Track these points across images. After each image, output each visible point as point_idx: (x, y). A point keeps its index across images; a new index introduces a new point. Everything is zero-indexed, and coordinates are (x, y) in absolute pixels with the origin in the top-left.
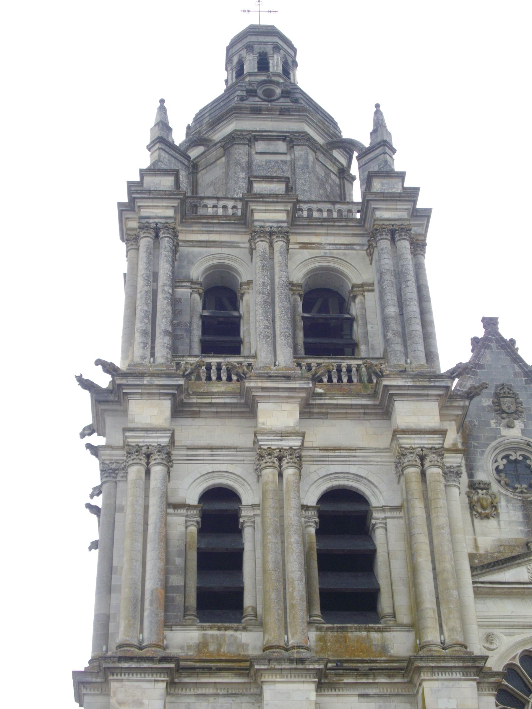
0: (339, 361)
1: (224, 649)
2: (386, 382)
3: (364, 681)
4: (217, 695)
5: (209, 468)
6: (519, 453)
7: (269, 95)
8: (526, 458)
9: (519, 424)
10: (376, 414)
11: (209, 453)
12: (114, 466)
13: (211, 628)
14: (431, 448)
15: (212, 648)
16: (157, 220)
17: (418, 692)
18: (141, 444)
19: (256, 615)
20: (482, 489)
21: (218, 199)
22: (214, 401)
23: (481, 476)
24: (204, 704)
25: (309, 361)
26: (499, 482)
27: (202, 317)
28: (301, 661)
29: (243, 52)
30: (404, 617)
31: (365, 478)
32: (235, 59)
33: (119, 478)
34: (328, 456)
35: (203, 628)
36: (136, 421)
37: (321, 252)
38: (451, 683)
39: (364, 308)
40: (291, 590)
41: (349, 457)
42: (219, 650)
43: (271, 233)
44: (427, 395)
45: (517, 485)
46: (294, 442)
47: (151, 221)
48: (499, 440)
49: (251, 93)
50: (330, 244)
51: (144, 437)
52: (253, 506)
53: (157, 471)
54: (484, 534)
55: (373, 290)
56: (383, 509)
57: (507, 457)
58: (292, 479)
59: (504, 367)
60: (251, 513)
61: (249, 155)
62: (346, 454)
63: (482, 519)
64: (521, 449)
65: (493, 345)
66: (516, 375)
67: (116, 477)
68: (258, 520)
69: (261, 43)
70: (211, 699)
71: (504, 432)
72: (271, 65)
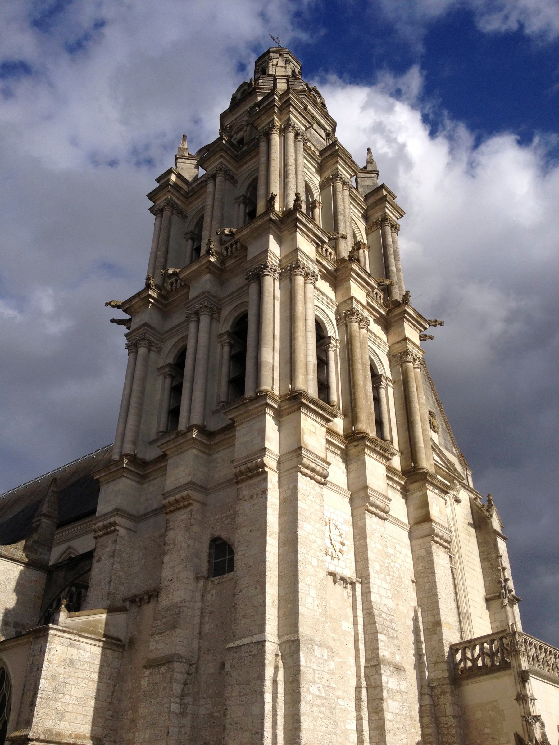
2: (407, 309)
22: (324, 263)
31: (378, 356)
40: (369, 403)
41: (374, 339)
44: (417, 328)
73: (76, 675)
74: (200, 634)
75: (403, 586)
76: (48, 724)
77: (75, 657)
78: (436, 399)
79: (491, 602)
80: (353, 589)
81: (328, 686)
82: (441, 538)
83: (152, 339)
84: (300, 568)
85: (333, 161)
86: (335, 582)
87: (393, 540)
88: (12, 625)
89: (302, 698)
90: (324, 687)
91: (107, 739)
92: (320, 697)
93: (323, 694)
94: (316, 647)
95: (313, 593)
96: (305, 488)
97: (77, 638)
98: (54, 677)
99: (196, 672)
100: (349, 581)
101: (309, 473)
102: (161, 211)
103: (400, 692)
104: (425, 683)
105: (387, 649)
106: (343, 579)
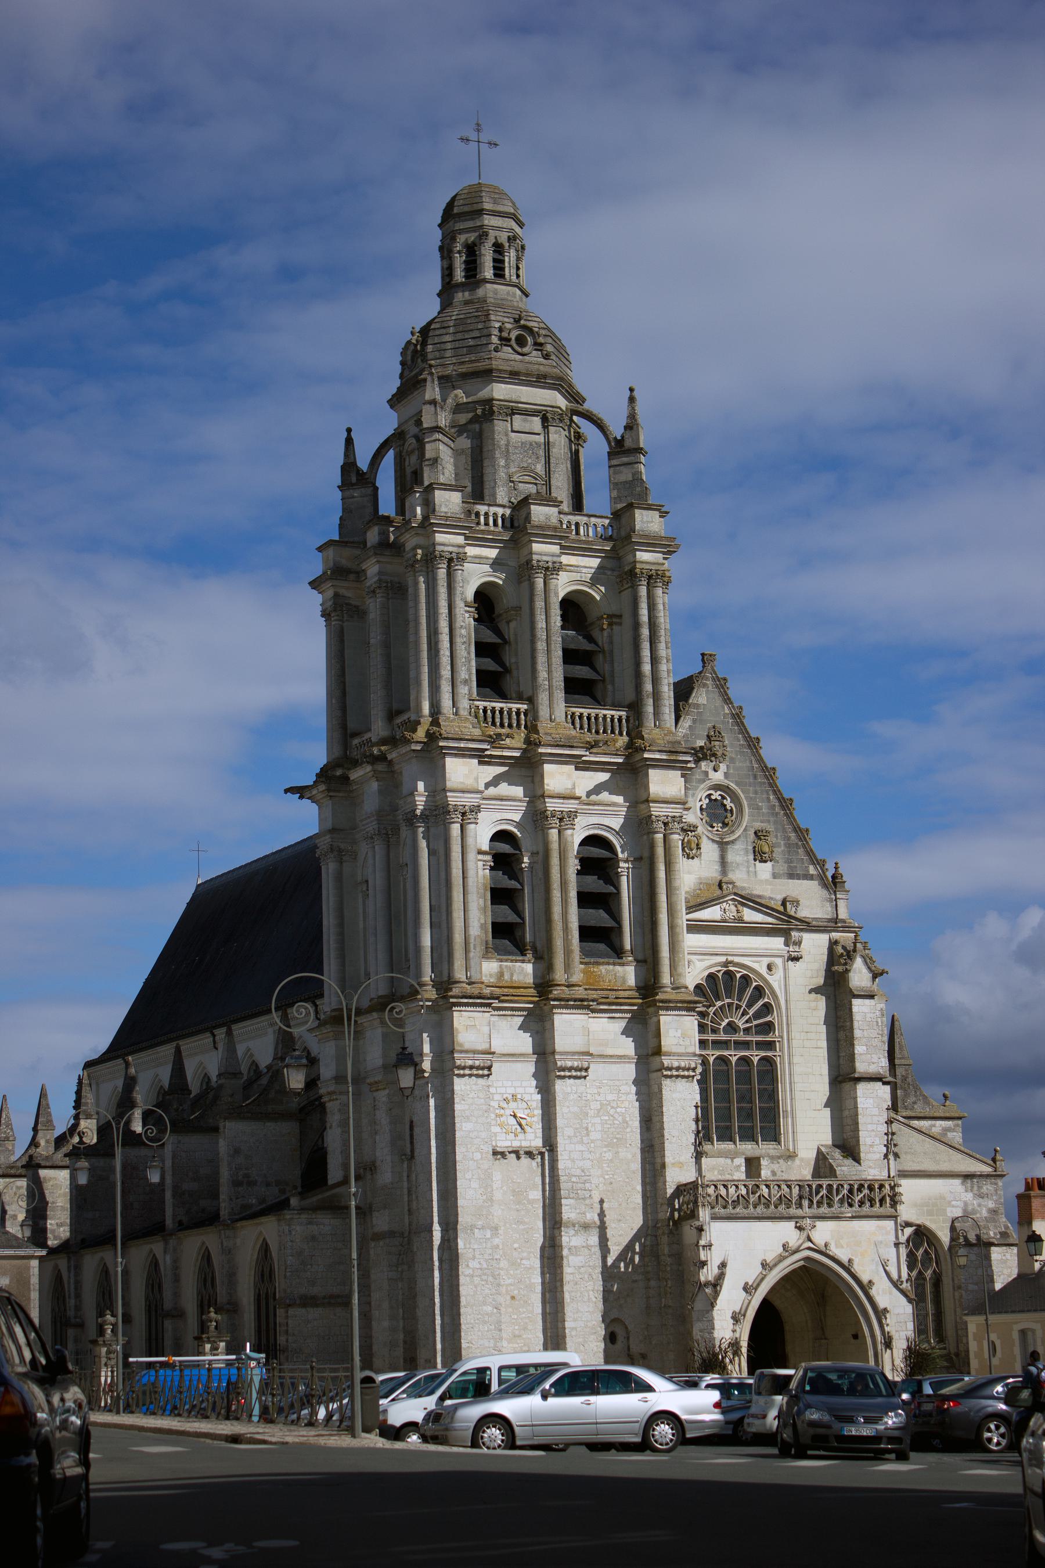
0: (597, 711)
1: (515, 978)
2: (646, 755)
3: (614, 1007)
6: (719, 793)
9: (723, 767)
10: (627, 769)
11: (499, 803)
13: (506, 961)
14: (674, 817)
15: (507, 977)
16: (450, 549)
17: (650, 1018)
20: (691, 831)
23: (692, 817)
26: (702, 820)
28: (582, 1000)
34: (589, 809)
37: (577, 576)
38: (678, 1018)
39: (611, 643)
42: (511, 979)
43: (547, 569)
45: (715, 825)
46: (571, 805)
47: (446, 549)
48: (707, 782)
49: (505, 341)
50: (585, 567)
51: (461, 797)
54: (689, 873)
55: (620, 624)
57: (710, 795)
61: (507, 435)
63: (688, 858)
64: (721, 790)
65: (709, 682)
66: (725, 715)
67: (427, 823)
71: (712, 775)
72: (507, 264)
74: (409, 1210)
75: (628, 1130)
78: (778, 799)
80: (543, 1158)
81: (492, 1259)
82: (678, 1069)
83: (342, 846)
84: (458, 1167)
85: (526, 539)
86: (518, 1158)
87: (617, 1083)
89: (460, 1273)
90: (486, 1261)
92: (481, 1269)
93: (485, 1266)
94: (476, 1231)
95: (475, 1184)
96: (463, 1088)
97: (314, 1216)
99: (409, 1243)
101: (467, 1072)
102: (329, 615)
103: (588, 1247)
105: (573, 1210)
106: (530, 1154)
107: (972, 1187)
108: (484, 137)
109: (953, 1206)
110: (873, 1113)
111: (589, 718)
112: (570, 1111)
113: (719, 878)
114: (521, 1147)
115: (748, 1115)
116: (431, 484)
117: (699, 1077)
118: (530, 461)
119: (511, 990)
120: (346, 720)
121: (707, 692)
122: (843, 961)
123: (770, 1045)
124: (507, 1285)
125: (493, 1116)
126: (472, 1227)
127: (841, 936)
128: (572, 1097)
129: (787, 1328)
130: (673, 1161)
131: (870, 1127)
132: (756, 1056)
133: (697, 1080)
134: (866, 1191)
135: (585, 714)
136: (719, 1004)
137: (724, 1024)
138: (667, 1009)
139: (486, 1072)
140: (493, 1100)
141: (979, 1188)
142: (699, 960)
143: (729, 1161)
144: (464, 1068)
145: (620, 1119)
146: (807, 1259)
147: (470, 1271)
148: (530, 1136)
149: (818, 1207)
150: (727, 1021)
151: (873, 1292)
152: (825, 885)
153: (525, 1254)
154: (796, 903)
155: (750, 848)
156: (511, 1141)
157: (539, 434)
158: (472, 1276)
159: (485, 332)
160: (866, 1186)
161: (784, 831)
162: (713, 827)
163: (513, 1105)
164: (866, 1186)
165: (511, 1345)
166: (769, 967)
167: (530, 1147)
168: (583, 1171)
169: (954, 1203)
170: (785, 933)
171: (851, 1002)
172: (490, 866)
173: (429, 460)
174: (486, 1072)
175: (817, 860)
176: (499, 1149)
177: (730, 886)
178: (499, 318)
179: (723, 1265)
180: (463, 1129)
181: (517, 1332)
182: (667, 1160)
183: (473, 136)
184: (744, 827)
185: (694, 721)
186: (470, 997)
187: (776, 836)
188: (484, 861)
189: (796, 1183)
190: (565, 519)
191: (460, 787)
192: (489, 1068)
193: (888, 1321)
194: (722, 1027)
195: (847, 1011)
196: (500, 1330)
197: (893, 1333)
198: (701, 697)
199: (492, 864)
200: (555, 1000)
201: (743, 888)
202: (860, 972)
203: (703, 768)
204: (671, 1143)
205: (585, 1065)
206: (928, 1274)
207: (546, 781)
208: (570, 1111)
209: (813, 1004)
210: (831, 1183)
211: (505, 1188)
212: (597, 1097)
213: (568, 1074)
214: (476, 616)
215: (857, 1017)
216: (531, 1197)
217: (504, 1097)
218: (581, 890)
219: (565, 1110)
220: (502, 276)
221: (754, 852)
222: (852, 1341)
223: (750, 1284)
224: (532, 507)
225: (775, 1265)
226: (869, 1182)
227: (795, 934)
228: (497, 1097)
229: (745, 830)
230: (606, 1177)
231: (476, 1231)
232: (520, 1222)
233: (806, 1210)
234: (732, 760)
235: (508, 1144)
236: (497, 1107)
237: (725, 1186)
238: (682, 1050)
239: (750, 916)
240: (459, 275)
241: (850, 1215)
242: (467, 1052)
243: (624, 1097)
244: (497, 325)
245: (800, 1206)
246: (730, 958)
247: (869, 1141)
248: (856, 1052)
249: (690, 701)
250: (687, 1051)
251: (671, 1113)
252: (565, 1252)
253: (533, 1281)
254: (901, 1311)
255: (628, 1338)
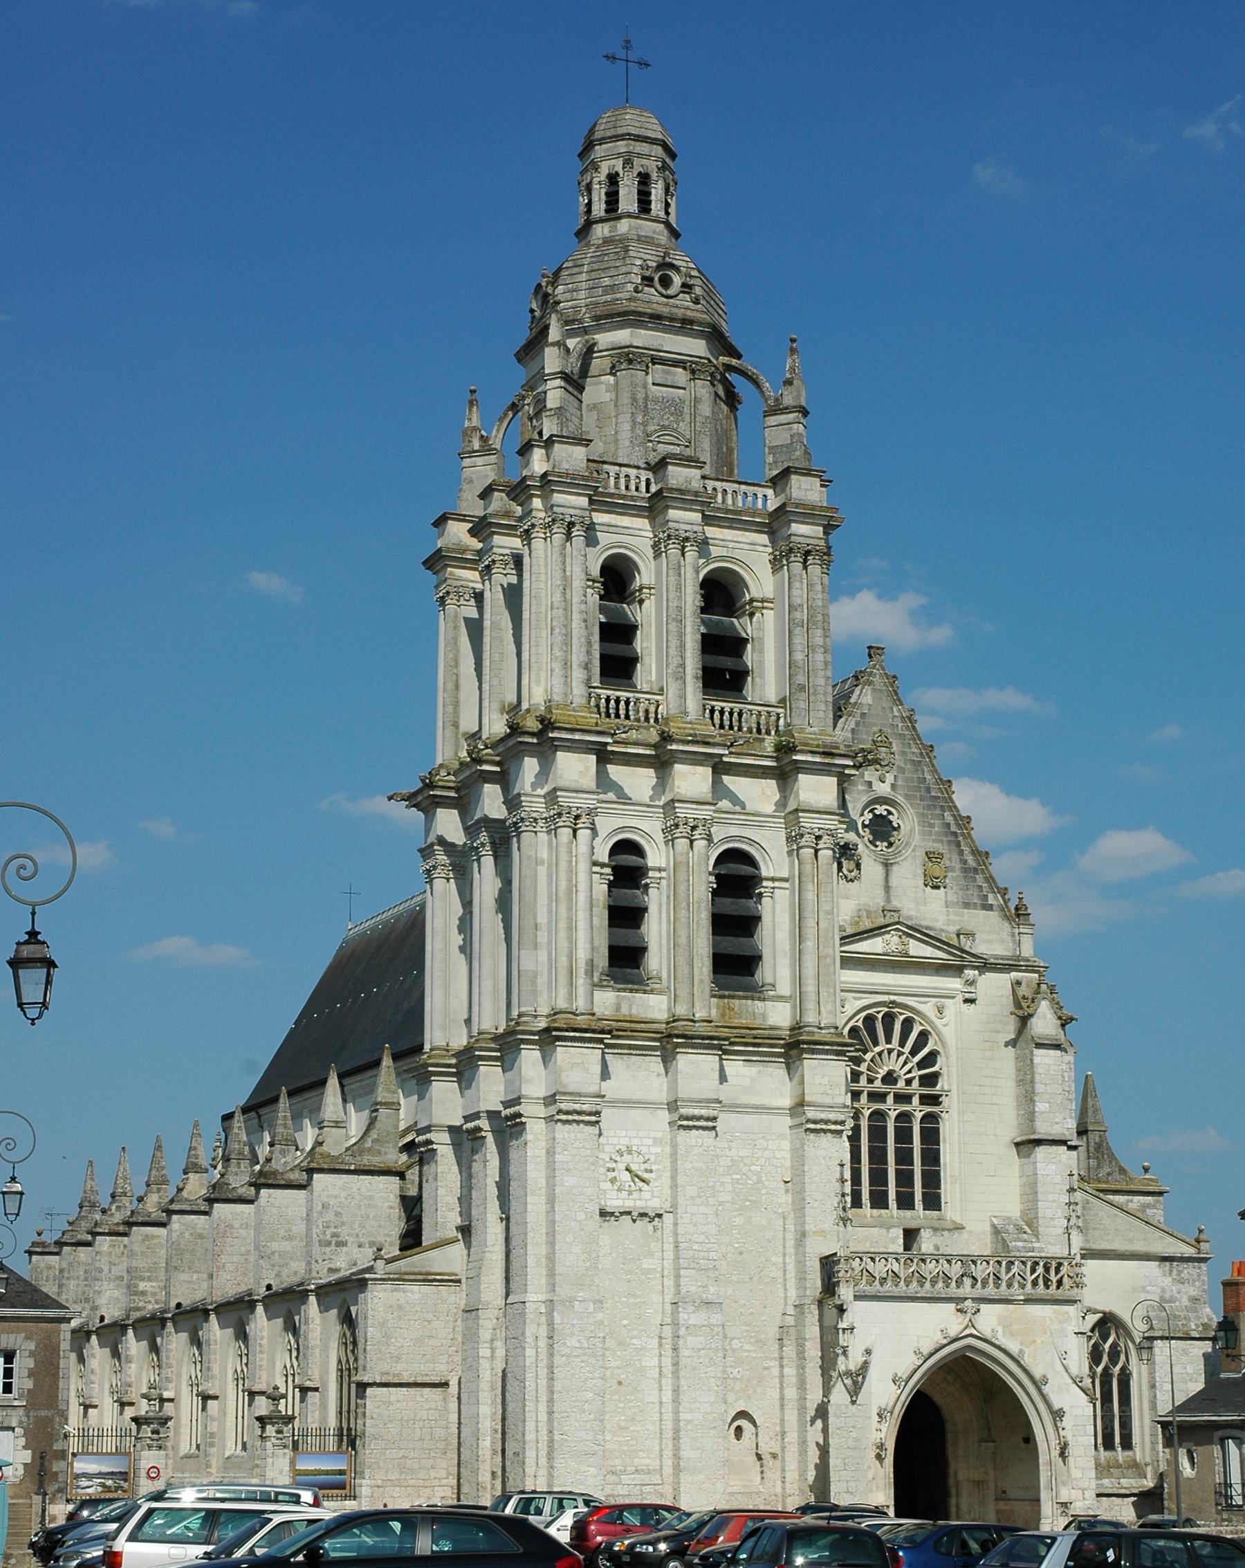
1: (634, 1011)
4: (631, 1054)
5: (621, 822)
7: (666, 282)
8: (890, 813)
12: (534, 815)
16: (572, 511)
18: (571, 805)
19: (660, 979)
21: (621, 465)
24: (620, 1061)
25: (714, 703)
27: (601, 623)
29: (618, 165)
30: (784, 988)
32: (605, 169)
33: (538, 829)
35: (619, 990)
36: (565, 777)
43: (687, 539)
45: (878, 843)
49: (648, 281)
52: (660, 870)
53: (584, 834)
56: (773, 879)
58: (703, 851)
59: (884, 708)
60: (657, 875)
61: (645, 387)
62: (745, 817)
64: (887, 804)
68: (664, 882)
69: (640, 156)
70: (625, 1057)
72: (653, 197)
73: (406, 1318)
75: (764, 1191)
76: (385, 1367)
77: (402, 1301)
78: (954, 816)
79: (1022, 1147)
88: (367, 1245)
91: (453, 1373)
92: (580, 1348)
98: (382, 1324)
100: (652, 1214)
103: (709, 1326)
104: (790, 1302)
107: (1171, 1271)
108: (633, 56)
109: (1148, 1292)
110: (1056, 1181)
111: (731, 714)
112: (693, 1167)
113: (882, 904)
114: (635, 1208)
115: (905, 1179)
116: (552, 436)
117: (850, 1133)
118: (672, 419)
119: (628, 1025)
120: (458, 717)
121: (874, 690)
122: (1024, 1004)
123: (934, 1100)
124: (613, 1368)
125: (603, 1170)
126: (571, 1301)
127: (1022, 977)
128: (696, 1151)
129: (948, 1427)
130: (815, 1229)
131: (1051, 1198)
132: (918, 1111)
133: (848, 1137)
134: (1040, 1270)
135: (727, 710)
136: (878, 1049)
137: (882, 1072)
138: (813, 1052)
139: (593, 1118)
140: (603, 1151)
141: (1180, 1272)
142: (855, 999)
143: (884, 1231)
144: (568, 1113)
145: (754, 1178)
146: (970, 1347)
147: (567, 1351)
148: (646, 1195)
149: (984, 1287)
150: (886, 1069)
151: (1046, 1389)
152: (1007, 918)
153: (635, 1333)
154: (970, 935)
155: (920, 872)
156: (623, 1199)
157: (684, 389)
158: (569, 1356)
159: (624, 269)
160: (1042, 1264)
161: (961, 853)
162: (877, 846)
163: (627, 1158)
164: (1042, 1264)
165: (615, 1439)
166: (940, 1010)
167: (646, 1208)
168: (707, 1238)
169: (1148, 1288)
170: (957, 970)
171: (1032, 1052)
172: (609, 880)
173: (551, 409)
174: (593, 1118)
175: (997, 888)
176: (609, 1210)
177: (896, 915)
178: (639, 255)
179: (868, 1352)
180: (566, 1182)
181: (623, 1424)
182: (807, 1227)
183: (621, 54)
184: (912, 847)
185: (857, 724)
186: (575, 1030)
187: (950, 859)
188: (602, 874)
189: (958, 1258)
190: (710, 484)
191: (574, 786)
192: (598, 1113)
193: (1064, 1424)
194: (880, 1076)
195: (1029, 1062)
196: (602, 1421)
197: (1069, 1439)
198: (864, 697)
199: (612, 878)
200: (678, 1036)
201: (910, 918)
202: (1045, 1017)
203: (866, 779)
204: (812, 1208)
205: (712, 1113)
206: (1117, 1370)
207: (676, 783)
208: (693, 1167)
209: (988, 1054)
210: (999, 1259)
211: (614, 1255)
212: (730, 1154)
213: (691, 1123)
214: (602, 592)
215: (1039, 1070)
216: (645, 1266)
217: (617, 1148)
218: (716, 911)
219: (688, 1166)
220: (648, 211)
221: (925, 876)
222: (1023, 1445)
223: (899, 1375)
224: (670, 467)
225: (931, 1355)
226: (1045, 1260)
227: (970, 973)
228: (607, 1149)
229: (913, 850)
230: (736, 1245)
231: (577, 1303)
232: (630, 1295)
233: (967, 1289)
234: (902, 770)
235: (620, 1203)
236: (608, 1159)
237: (873, 1259)
238: (827, 1100)
239: (917, 949)
240: (599, 209)
241: (1022, 1298)
242: (571, 1094)
243: (759, 1154)
244: (639, 262)
245: (959, 1283)
246: (892, 998)
247: (1049, 1213)
248: (1037, 1109)
249: (852, 700)
250: (835, 1101)
251: (814, 1173)
252: (682, 1332)
253: (644, 1364)
254: (1080, 1412)
255: (757, 1434)
